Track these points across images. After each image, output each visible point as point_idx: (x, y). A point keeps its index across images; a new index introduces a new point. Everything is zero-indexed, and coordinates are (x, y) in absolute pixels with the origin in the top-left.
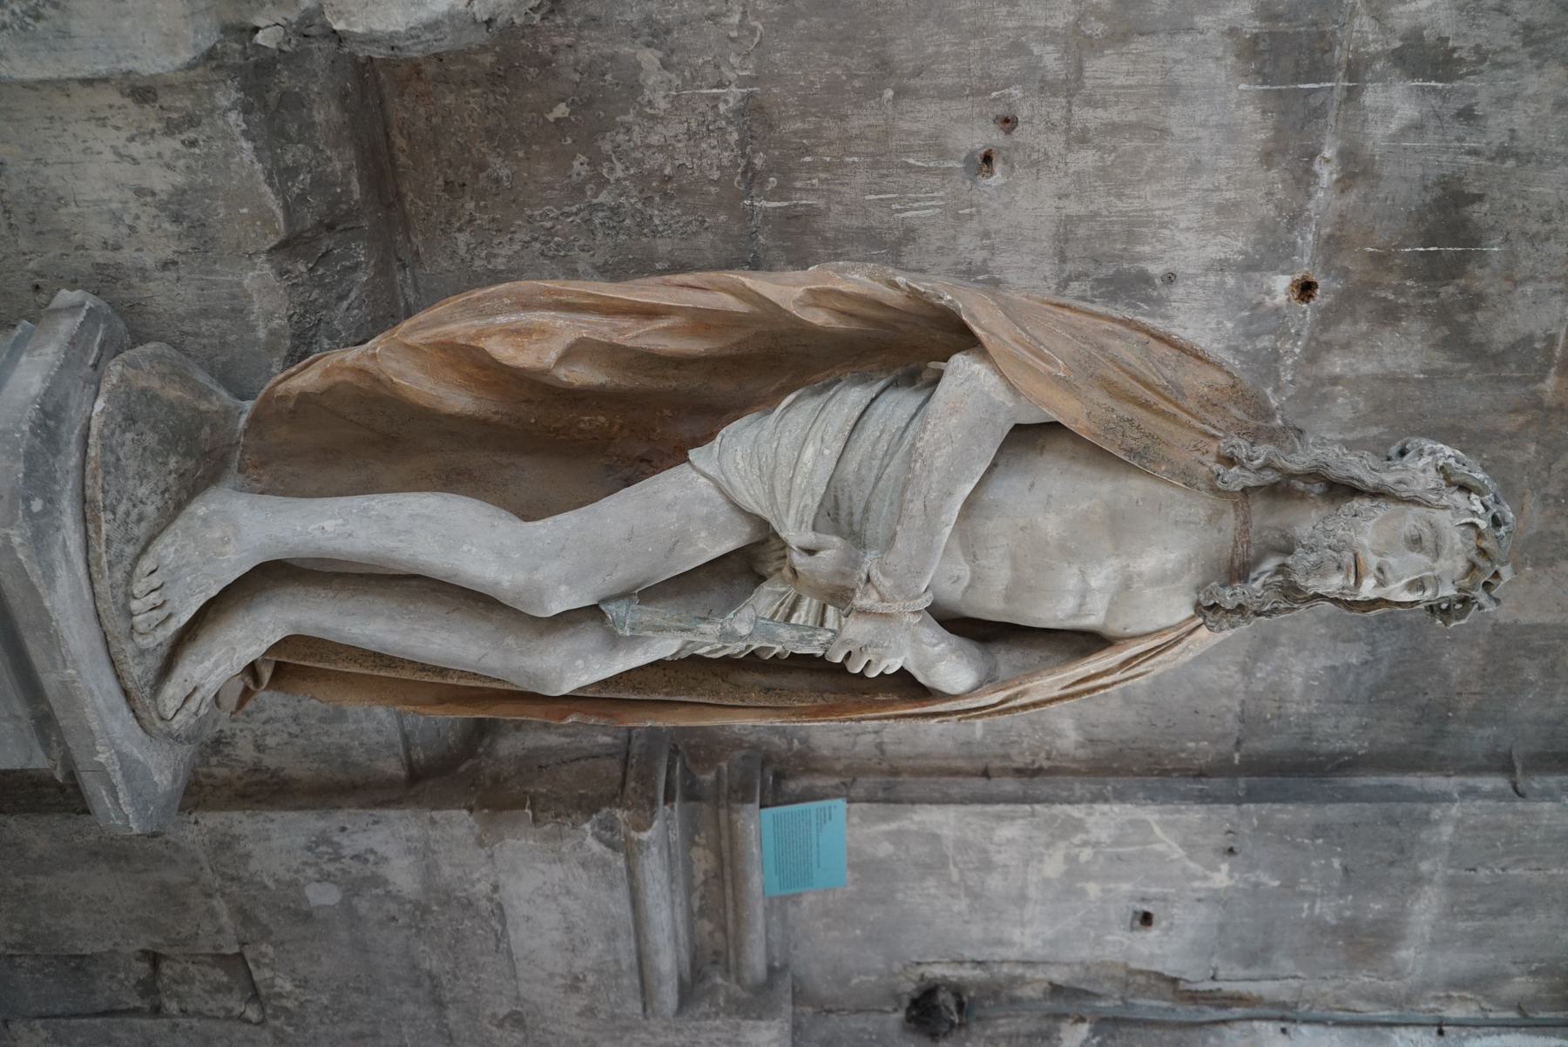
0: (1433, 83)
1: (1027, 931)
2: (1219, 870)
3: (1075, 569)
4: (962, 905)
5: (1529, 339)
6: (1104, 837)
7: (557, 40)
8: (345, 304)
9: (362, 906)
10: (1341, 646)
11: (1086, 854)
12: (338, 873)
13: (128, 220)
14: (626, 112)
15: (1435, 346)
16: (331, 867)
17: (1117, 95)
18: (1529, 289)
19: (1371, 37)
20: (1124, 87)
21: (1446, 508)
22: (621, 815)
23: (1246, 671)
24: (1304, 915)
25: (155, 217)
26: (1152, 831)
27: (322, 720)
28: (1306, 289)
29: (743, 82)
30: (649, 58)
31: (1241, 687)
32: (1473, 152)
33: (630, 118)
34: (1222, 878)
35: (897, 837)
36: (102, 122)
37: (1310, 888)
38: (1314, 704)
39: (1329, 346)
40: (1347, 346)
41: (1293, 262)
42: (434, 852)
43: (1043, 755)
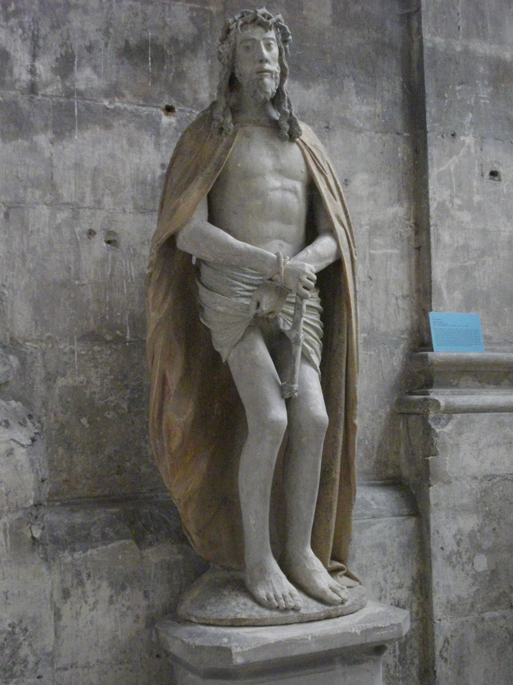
0: (76, 62)
1: (502, 229)
2: (464, 141)
3: (271, 193)
4: (489, 260)
5: (192, 18)
6: (448, 193)
7: (52, 420)
8: (169, 520)
9: (487, 544)
10: (346, 89)
11: (457, 201)
12: (468, 554)
13: (124, 610)
14: (86, 393)
15: (196, 56)
16: (465, 558)
17: (79, 188)
18: (168, 19)
19: (55, 88)
20: (76, 185)
21: (236, 38)
22: (432, 415)
23: (360, 131)
24: (488, 102)
25: (123, 597)
26: (444, 171)
27: (384, 554)
28: (169, 110)
29: (72, 343)
30: (61, 382)
31: (368, 133)
32: (106, 45)
33: (88, 392)
34: (468, 139)
35: (450, 288)
36: (78, 614)
37: (473, 100)
38: (376, 101)
39: (196, 100)
40: (195, 92)
41: (156, 115)
42: (455, 506)
43: (407, 222)
